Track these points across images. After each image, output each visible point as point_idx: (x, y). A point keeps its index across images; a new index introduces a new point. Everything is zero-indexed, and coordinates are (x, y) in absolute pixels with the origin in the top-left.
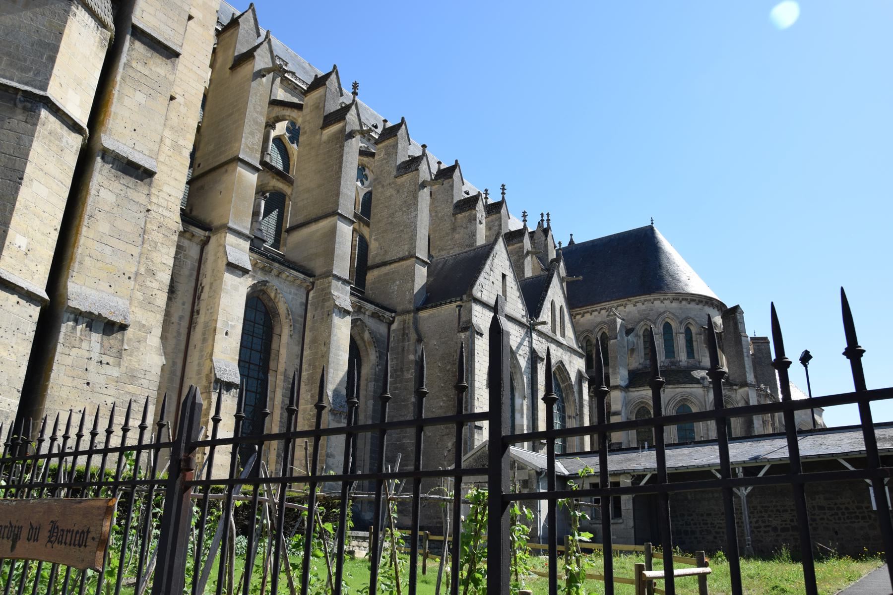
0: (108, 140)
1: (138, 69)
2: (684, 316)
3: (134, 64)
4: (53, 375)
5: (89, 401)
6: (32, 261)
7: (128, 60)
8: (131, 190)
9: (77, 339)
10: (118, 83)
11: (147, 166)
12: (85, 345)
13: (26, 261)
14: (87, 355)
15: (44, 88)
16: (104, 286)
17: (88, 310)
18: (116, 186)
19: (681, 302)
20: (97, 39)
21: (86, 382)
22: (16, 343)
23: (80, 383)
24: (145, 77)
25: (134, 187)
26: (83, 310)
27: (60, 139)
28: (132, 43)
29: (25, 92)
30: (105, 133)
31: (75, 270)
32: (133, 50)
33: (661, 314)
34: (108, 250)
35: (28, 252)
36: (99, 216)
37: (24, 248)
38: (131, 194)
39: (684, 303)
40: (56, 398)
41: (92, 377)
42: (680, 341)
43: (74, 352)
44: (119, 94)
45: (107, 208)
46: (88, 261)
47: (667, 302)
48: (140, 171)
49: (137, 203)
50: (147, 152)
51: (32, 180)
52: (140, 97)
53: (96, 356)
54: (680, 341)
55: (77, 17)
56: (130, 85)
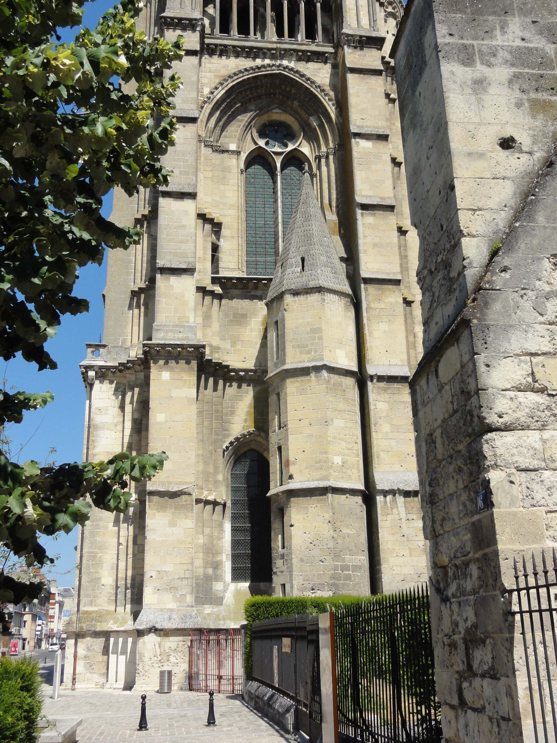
0: (371, 370)
1: (376, 307)
3: (372, 305)
4: (380, 535)
5: (407, 547)
6: (348, 469)
7: (367, 305)
8: (396, 395)
9: (389, 508)
10: (366, 324)
11: (402, 375)
12: (395, 511)
13: (344, 470)
14: (398, 517)
15: (322, 359)
16: (397, 467)
17: (390, 488)
18: (386, 396)
20: (343, 305)
21: (402, 535)
22: (353, 522)
23: (398, 536)
24: (382, 310)
25: (397, 392)
26: (387, 489)
27: (340, 385)
28: (366, 290)
29: (313, 367)
30: (368, 362)
31: (376, 463)
32: (368, 295)
34: (393, 443)
35: (344, 465)
36: (380, 421)
37: (340, 463)
38: (397, 397)
40: (386, 550)
41: (405, 531)
43: (389, 517)
44: (369, 332)
45: (385, 414)
46: (383, 455)
48: (399, 379)
49: (403, 402)
50: (399, 363)
51: (333, 420)
52: (383, 326)
53: (403, 516)
55: (326, 301)
56: (374, 321)
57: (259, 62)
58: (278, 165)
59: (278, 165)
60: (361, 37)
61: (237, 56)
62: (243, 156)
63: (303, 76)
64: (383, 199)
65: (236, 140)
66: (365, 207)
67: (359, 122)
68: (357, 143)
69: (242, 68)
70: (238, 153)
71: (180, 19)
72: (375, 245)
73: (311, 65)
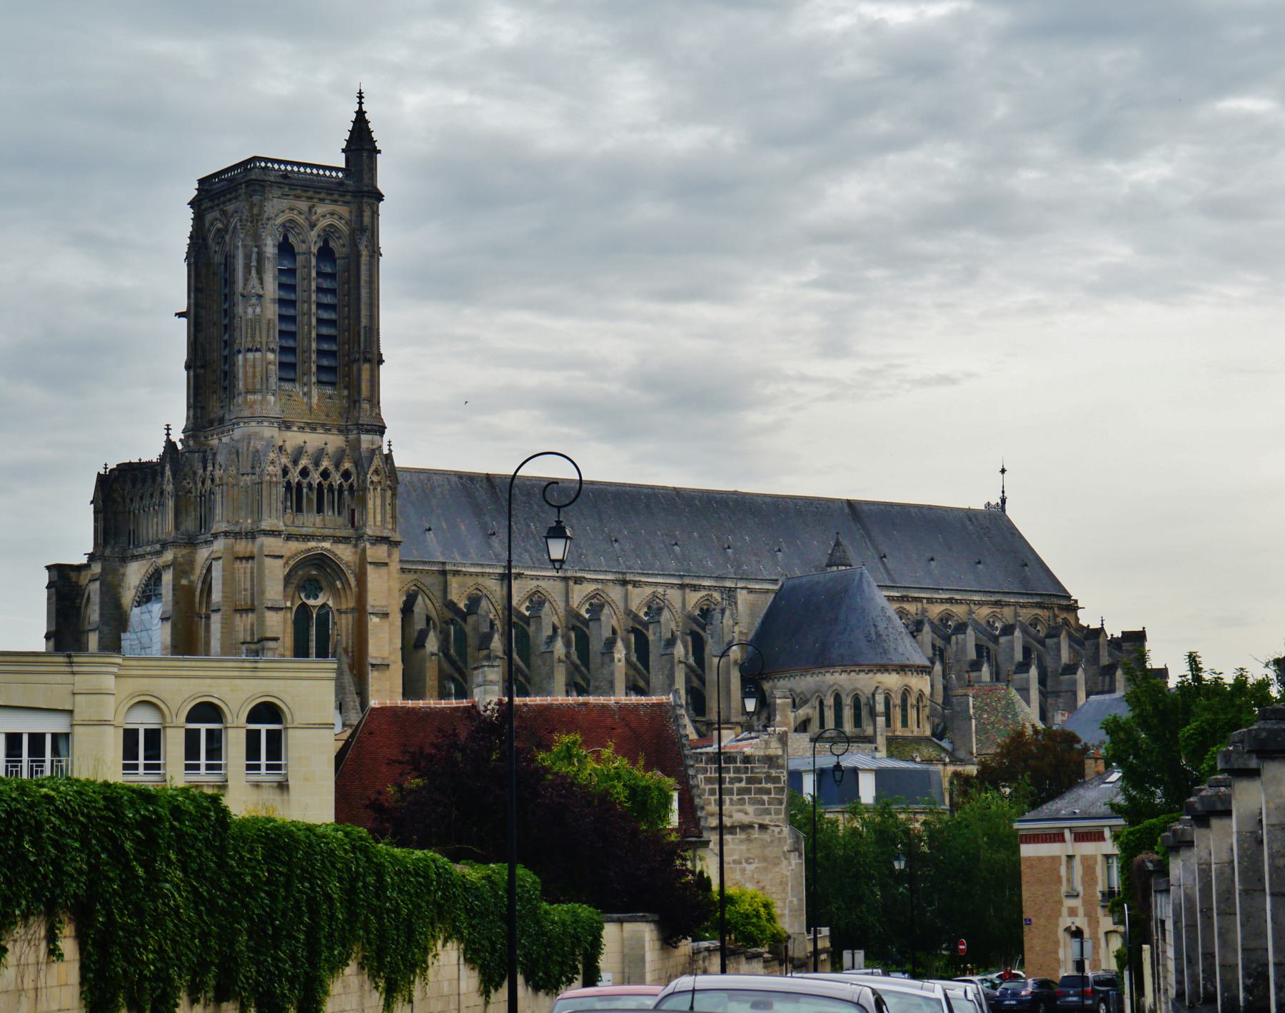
2: (851, 687)
19: (849, 674)
33: (831, 686)
39: (853, 674)
42: (848, 713)
47: (836, 675)
54: (848, 713)
57: (312, 544)
58: (314, 616)
59: (314, 616)
60: (378, 537)
61: (297, 540)
62: (295, 608)
63: (336, 555)
64: (383, 659)
65: (290, 599)
66: (373, 665)
67: (373, 606)
68: (371, 619)
69: (300, 549)
70: (291, 608)
71: (273, 531)
72: (377, 691)
73: (341, 546)
